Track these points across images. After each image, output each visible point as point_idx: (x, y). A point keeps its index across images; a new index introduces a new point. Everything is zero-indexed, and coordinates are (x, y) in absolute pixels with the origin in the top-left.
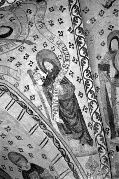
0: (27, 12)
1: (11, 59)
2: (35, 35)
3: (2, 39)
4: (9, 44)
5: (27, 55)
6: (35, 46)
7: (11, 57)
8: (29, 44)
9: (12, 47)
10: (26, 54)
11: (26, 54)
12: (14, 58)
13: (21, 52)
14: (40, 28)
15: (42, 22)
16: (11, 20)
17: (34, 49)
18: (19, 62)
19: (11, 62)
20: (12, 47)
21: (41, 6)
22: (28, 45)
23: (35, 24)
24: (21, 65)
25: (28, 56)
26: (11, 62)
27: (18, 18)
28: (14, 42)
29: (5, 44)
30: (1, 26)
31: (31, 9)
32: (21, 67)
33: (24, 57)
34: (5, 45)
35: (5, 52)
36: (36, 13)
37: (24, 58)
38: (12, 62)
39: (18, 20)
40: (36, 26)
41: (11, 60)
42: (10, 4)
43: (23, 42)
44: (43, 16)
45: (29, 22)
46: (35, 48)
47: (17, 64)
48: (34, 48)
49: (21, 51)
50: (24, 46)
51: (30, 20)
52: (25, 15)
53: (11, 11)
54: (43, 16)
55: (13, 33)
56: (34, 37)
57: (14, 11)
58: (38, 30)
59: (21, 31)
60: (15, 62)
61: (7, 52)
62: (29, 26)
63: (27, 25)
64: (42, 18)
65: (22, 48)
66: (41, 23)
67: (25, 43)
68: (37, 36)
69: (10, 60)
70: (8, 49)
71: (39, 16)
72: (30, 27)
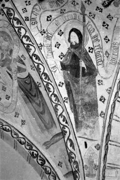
0: (50, 20)
1: (105, 25)
2: (73, 5)
3: (83, 38)
4: (88, 29)
5: (98, 9)
6: (85, 3)
7: (103, 26)
8: (85, 8)
9: (91, 26)
10: (96, 10)
11: (96, 10)
12: (104, 23)
13: (96, 16)
14: (64, 1)
15: (57, 2)
16: (61, 34)
17: (88, 2)
18: (108, 17)
19: (108, 25)
20: (91, 26)
21: (40, 9)
22: (86, 9)
23: (62, 7)
24: (110, 14)
25: (98, 7)
26: (108, 25)
27: (58, 27)
28: (86, 24)
29: (89, 34)
30: (68, 42)
31: (47, 18)
32: (112, 15)
33: (100, 11)
34: (90, 33)
35: (98, 33)
36: (48, 10)
37: (101, 11)
38: (108, 24)
39: (61, 26)
40: (63, 6)
41: (106, 25)
42: (35, 49)
43: (84, 15)
44: (50, 3)
45: (61, 14)
46: (87, 2)
47: (110, 19)
48: (87, 3)
49: (95, 15)
50: (89, 13)
51: (59, 14)
52: (54, 20)
53: (52, 38)
54: (50, 3)
55: (76, 28)
56: (75, 5)
57: (51, 34)
58: (66, 3)
59: (74, 19)
60: (108, 22)
61: (98, 30)
62: (66, 13)
63: (65, 15)
64: (52, 3)
65: (91, 15)
66: (58, 2)
67: (84, 12)
68: (73, 3)
69: (106, 26)
70: (94, 29)
71: (51, 6)
72: (66, 11)
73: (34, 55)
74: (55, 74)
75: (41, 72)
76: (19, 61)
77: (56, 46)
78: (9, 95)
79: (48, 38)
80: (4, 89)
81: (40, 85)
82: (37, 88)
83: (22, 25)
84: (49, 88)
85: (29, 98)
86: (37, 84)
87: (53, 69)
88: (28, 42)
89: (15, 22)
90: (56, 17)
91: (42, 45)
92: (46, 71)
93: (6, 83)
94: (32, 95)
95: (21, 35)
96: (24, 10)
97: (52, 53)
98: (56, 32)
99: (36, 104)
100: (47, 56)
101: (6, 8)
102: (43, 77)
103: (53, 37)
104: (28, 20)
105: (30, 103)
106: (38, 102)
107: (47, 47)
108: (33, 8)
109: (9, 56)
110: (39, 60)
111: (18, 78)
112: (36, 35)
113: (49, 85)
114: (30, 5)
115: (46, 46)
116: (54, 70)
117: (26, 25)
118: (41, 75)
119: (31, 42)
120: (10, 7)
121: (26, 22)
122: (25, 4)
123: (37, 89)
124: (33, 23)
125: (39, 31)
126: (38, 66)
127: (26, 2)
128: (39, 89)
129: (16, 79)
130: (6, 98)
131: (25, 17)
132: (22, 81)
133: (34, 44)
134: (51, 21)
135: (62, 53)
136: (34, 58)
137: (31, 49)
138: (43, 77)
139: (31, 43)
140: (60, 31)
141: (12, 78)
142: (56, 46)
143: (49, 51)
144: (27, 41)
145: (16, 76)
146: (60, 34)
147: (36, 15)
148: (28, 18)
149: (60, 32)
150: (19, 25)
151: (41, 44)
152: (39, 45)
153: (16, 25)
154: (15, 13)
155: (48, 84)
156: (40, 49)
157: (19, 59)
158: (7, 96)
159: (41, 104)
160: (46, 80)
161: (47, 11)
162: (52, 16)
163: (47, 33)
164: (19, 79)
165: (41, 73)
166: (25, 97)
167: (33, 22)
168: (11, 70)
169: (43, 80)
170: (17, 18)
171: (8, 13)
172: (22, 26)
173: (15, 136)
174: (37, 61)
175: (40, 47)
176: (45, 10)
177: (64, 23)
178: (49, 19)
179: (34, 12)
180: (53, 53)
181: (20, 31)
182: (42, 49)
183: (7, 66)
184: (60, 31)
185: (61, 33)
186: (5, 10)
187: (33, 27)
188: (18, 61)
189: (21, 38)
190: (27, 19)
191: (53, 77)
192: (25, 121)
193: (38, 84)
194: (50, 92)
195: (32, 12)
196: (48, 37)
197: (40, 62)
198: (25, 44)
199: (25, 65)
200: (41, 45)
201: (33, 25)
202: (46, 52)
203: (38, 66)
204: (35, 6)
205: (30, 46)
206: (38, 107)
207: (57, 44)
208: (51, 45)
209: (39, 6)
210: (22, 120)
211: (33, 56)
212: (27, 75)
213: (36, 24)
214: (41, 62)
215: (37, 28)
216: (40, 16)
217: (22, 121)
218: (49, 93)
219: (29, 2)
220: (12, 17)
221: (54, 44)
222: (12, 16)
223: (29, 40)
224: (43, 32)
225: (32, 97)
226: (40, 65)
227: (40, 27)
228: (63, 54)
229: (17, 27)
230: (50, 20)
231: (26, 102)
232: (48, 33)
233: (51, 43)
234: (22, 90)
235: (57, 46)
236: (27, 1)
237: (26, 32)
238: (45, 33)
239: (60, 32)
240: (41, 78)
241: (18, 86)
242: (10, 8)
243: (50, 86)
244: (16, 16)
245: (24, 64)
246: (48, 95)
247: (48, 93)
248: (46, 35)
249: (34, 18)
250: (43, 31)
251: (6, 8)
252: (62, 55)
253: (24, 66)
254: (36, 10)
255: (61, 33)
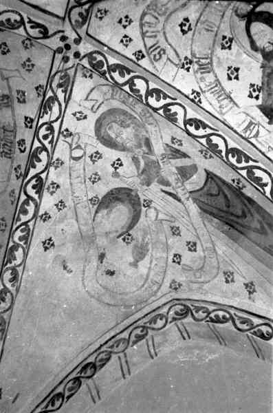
0: (190, 29)
21: (157, 18)
27: (214, 34)
31: (179, 28)
36: (175, 11)
42: (184, 108)
52: (199, 24)
53: (211, 63)
57: (207, 58)
73: (188, 122)
74: (259, 139)
75: (221, 151)
76: (173, 155)
77: (230, 79)
78: (192, 239)
79: (205, 68)
80: (175, 231)
81: (240, 185)
82: (238, 192)
83: (133, 72)
84: (257, 178)
85: (235, 224)
86: (235, 185)
87: (248, 132)
88: (162, 102)
89: (116, 75)
90: (198, 15)
91: (198, 93)
92: (232, 144)
93: (172, 217)
94: (238, 217)
95: (141, 96)
96: (124, 40)
97: (229, 97)
98: (216, 46)
99: (256, 230)
100: (221, 110)
101: (84, 57)
102: (233, 160)
103: (215, 60)
104: (143, 56)
105: (243, 237)
106: (256, 225)
107: (211, 91)
108: (142, 25)
109: (148, 156)
110: (205, 126)
111: (191, 192)
112: (173, 80)
113: (255, 170)
114: (132, 24)
115: (208, 91)
116: (254, 132)
117: (145, 69)
118: (225, 158)
119: (168, 99)
120: (90, 51)
121: (140, 62)
122: (120, 27)
123: (239, 198)
124: (158, 57)
125: (176, 65)
126: (209, 141)
127: (120, 22)
128: (243, 194)
129: (188, 199)
130: (190, 250)
131: (135, 54)
132: (201, 196)
133: (175, 99)
134: (191, 30)
135: (251, 84)
136: (192, 129)
137: (176, 113)
138: (233, 160)
139: (168, 101)
140: (223, 40)
141: (179, 200)
142: (230, 79)
143: (219, 97)
144: (158, 100)
145: (185, 191)
146: (227, 46)
147: (155, 36)
148: (140, 52)
149: (224, 42)
150: (127, 77)
151: (194, 92)
152: (192, 97)
153: (121, 80)
154: (107, 55)
155: (250, 170)
156: (199, 103)
157: (172, 151)
158: (190, 242)
159: (266, 226)
160: (244, 164)
161: (173, 15)
162: (190, 19)
163: (197, 60)
164: (194, 194)
165: (223, 154)
166: (226, 227)
167: (155, 56)
168: (168, 184)
169: (237, 167)
170: (114, 64)
171: (93, 66)
172: (132, 74)
173: (245, 327)
174: (201, 132)
175: (196, 98)
176: (167, 14)
177: (223, 16)
178: (186, 28)
179: (147, 32)
180: (232, 96)
181: (134, 88)
182: (202, 101)
183: (156, 180)
184: (223, 40)
185: (227, 43)
186: (85, 62)
187: (159, 65)
188: (170, 156)
189: (144, 102)
190: (140, 55)
191: (257, 148)
192: (252, 283)
193: (236, 183)
194: (265, 188)
195: (143, 35)
196: (203, 69)
197: (209, 131)
198: (157, 109)
199: (189, 157)
200: (195, 94)
201: (157, 60)
202: (214, 102)
203: (209, 141)
204: (142, 19)
205: (169, 107)
206: (263, 236)
207: (229, 72)
208: (218, 80)
209: (150, 14)
210: (244, 284)
211: (188, 126)
212: (204, 175)
213: (163, 55)
214: (211, 128)
215: (169, 62)
216: (164, 33)
217: (246, 285)
218: (263, 189)
219: (127, 17)
220: (105, 68)
221: (223, 76)
222: (103, 66)
223: (162, 96)
224: (186, 64)
225: (240, 221)
226: (212, 137)
227: (175, 56)
228: (255, 87)
229: (125, 84)
230: (190, 29)
231: (233, 240)
232: (199, 58)
233: (216, 77)
234: (211, 214)
235: (233, 77)
236: (121, 19)
237: (147, 82)
238: (191, 62)
239: (224, 42)
240: (232, 166)
241: (200, 211)
242: (91, 53)
243: (258, 173)
244: (112, 61)
245: (185, 155)
246: (264, 194)
247: (262, 191)
248: (196, 67)
249: (154, 46)
250: (185, 62)
251: (84, 57)
252: (254, 91)
253: (187, 159)
254: (150, 27)
255: (227, 44)
